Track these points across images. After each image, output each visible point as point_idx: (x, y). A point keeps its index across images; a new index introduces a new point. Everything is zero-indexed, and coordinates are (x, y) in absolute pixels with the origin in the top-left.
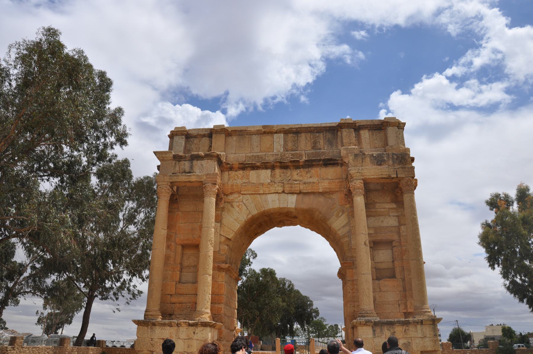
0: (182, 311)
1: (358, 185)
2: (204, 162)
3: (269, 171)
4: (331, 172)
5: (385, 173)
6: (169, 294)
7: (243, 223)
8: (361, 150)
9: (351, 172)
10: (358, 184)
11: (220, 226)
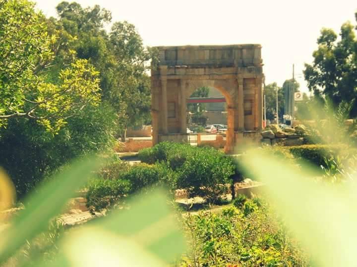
2: (181, 70)
3: (203, 70)
4: (230, 70)
10: (241, 81)
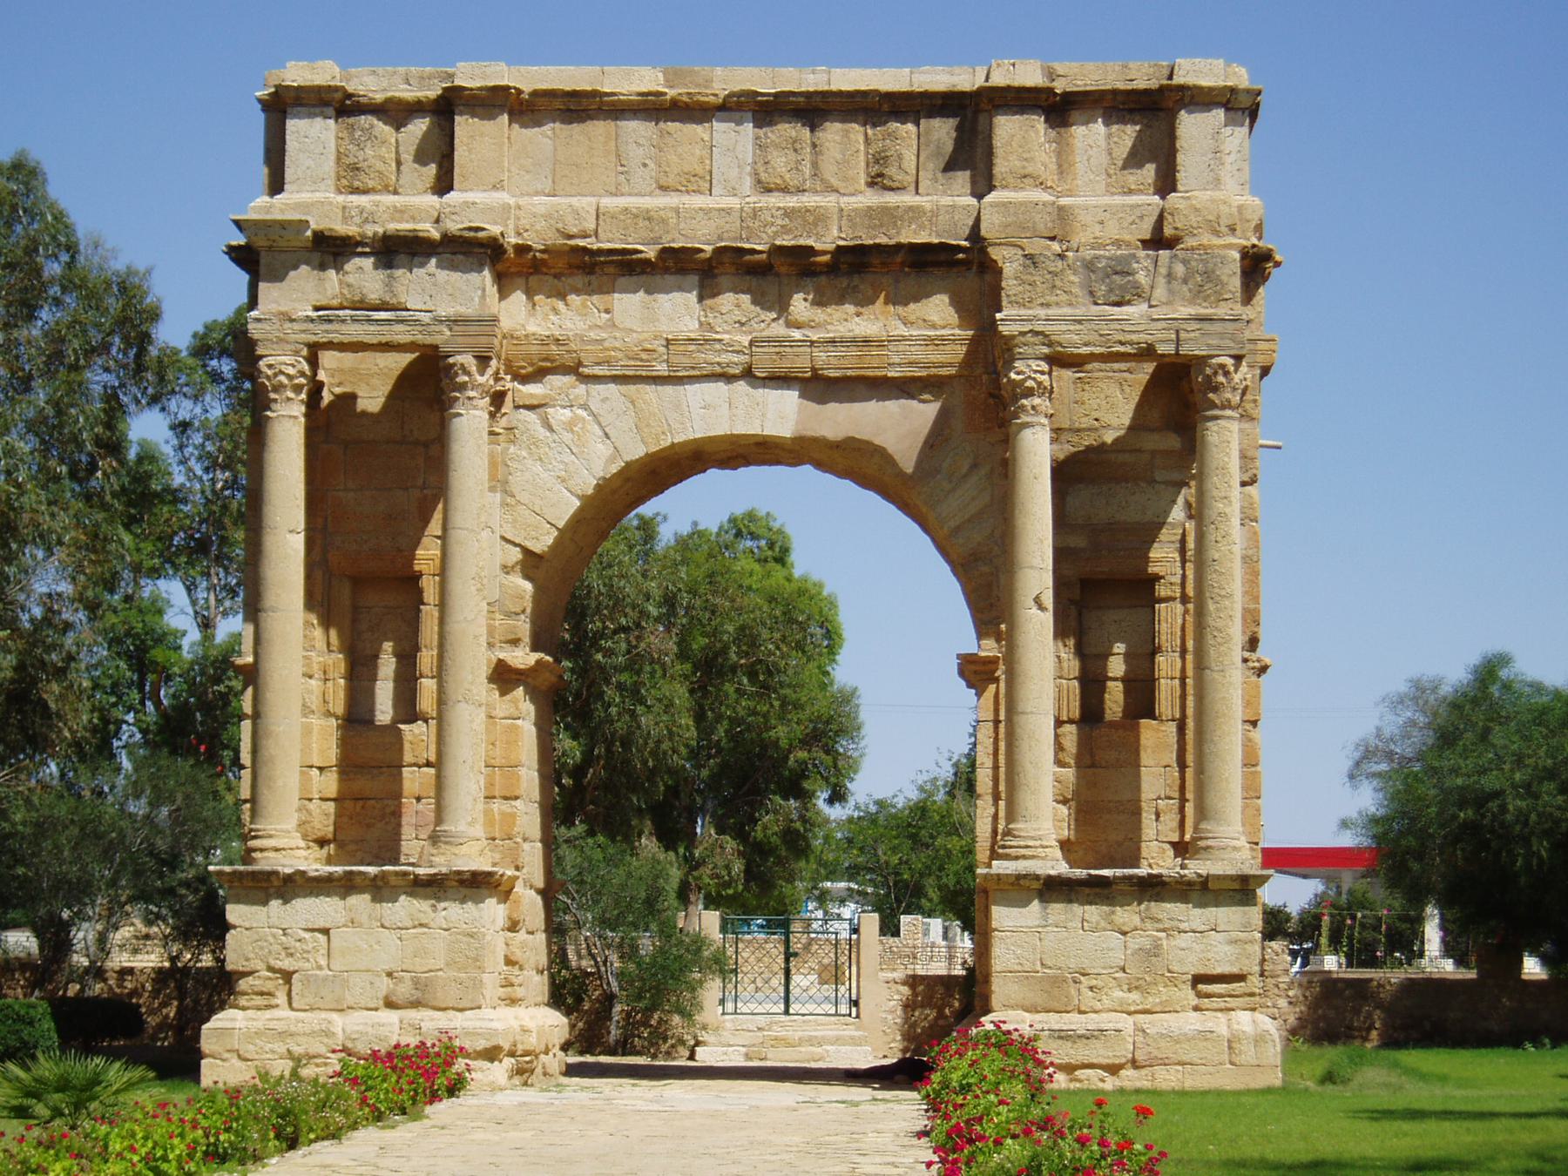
0: (369, 826)
1: (1030, 383)
5: (1134, 337)
6: (311, 767)
7: (590, 491)
8: (1064, 201)
9: (1005, 329)
11: (504, 504)
